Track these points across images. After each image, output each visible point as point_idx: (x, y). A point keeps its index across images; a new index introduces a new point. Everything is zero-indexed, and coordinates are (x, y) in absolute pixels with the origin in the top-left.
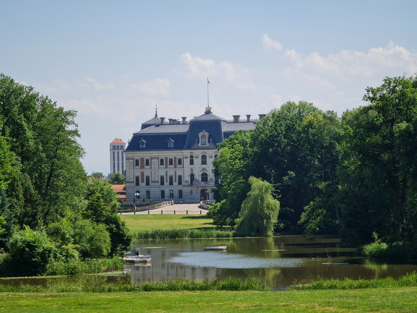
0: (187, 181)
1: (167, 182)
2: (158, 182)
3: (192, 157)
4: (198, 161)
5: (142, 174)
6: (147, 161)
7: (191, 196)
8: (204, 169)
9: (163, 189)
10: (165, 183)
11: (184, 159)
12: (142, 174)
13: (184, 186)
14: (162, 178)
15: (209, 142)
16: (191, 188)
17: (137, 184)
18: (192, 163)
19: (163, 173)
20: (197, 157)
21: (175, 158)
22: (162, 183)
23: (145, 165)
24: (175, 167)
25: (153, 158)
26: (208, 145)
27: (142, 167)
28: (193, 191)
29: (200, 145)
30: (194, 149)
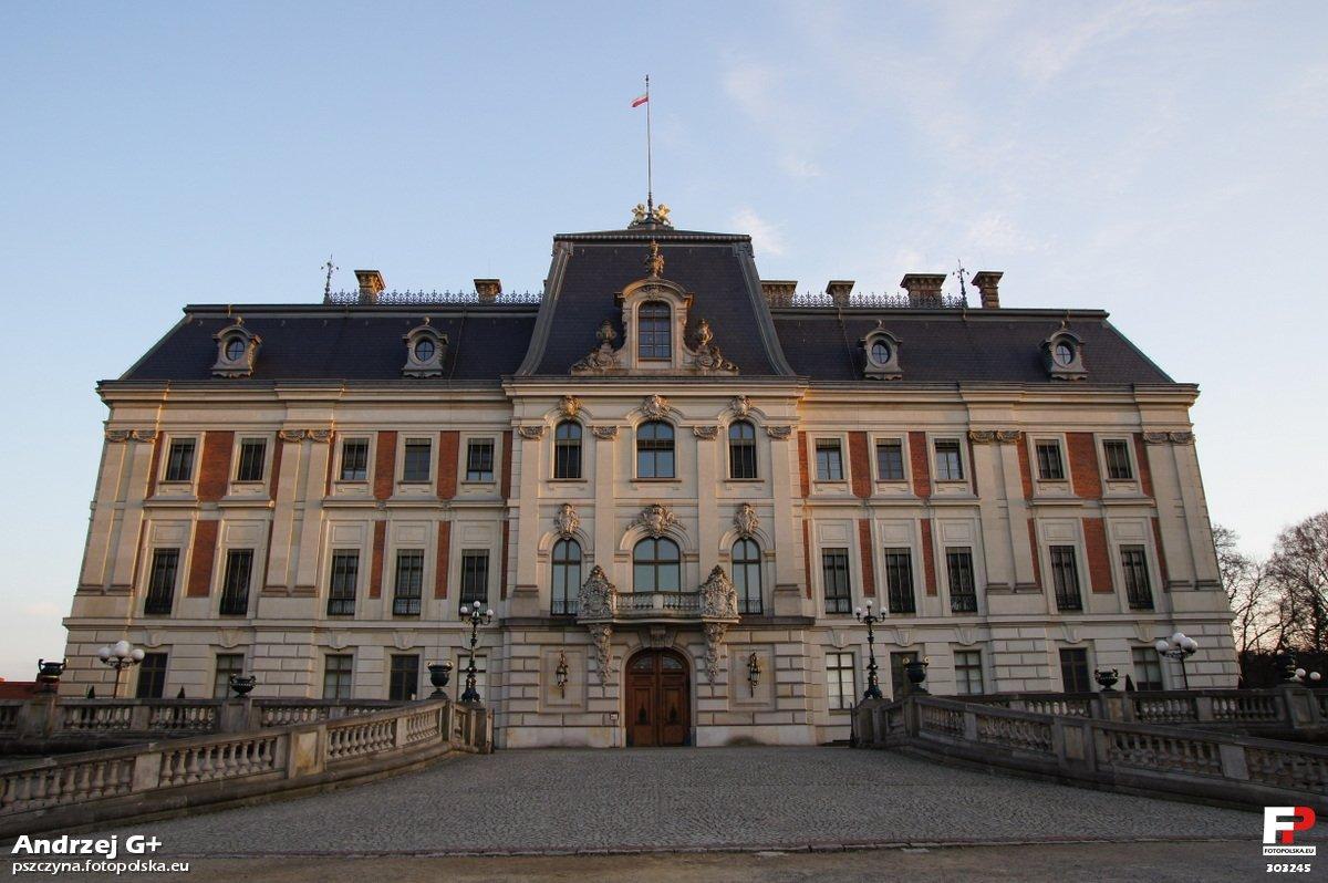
0: (529, 592)
1: (376, 591)
2: (309, 591)
3: (569, 422)
4: (612, 460)
5: (207, 533)
6: (254, 451)
7: (554, 698)
8: (652, 509)
9: (342, 641)
10: (364, 605)
11: (516, 444)
12: (207, 533)
13: (505, 625)
14: (344, 565)
15: (692, 341)
16: (556, 637)
17: (159, 602)
18: (568, 463)
19: (353, 532)
20: (606, 434)
21: (450, 439)
22: (341, 601)
23: (234, 475)
24: (447, 491)
25: (302, 436)
26: (681, 356)
27: (213, 490)
28: (575, 660)
29: (629, 358)
30: (584, 379)
